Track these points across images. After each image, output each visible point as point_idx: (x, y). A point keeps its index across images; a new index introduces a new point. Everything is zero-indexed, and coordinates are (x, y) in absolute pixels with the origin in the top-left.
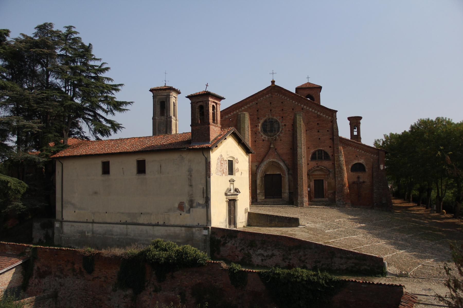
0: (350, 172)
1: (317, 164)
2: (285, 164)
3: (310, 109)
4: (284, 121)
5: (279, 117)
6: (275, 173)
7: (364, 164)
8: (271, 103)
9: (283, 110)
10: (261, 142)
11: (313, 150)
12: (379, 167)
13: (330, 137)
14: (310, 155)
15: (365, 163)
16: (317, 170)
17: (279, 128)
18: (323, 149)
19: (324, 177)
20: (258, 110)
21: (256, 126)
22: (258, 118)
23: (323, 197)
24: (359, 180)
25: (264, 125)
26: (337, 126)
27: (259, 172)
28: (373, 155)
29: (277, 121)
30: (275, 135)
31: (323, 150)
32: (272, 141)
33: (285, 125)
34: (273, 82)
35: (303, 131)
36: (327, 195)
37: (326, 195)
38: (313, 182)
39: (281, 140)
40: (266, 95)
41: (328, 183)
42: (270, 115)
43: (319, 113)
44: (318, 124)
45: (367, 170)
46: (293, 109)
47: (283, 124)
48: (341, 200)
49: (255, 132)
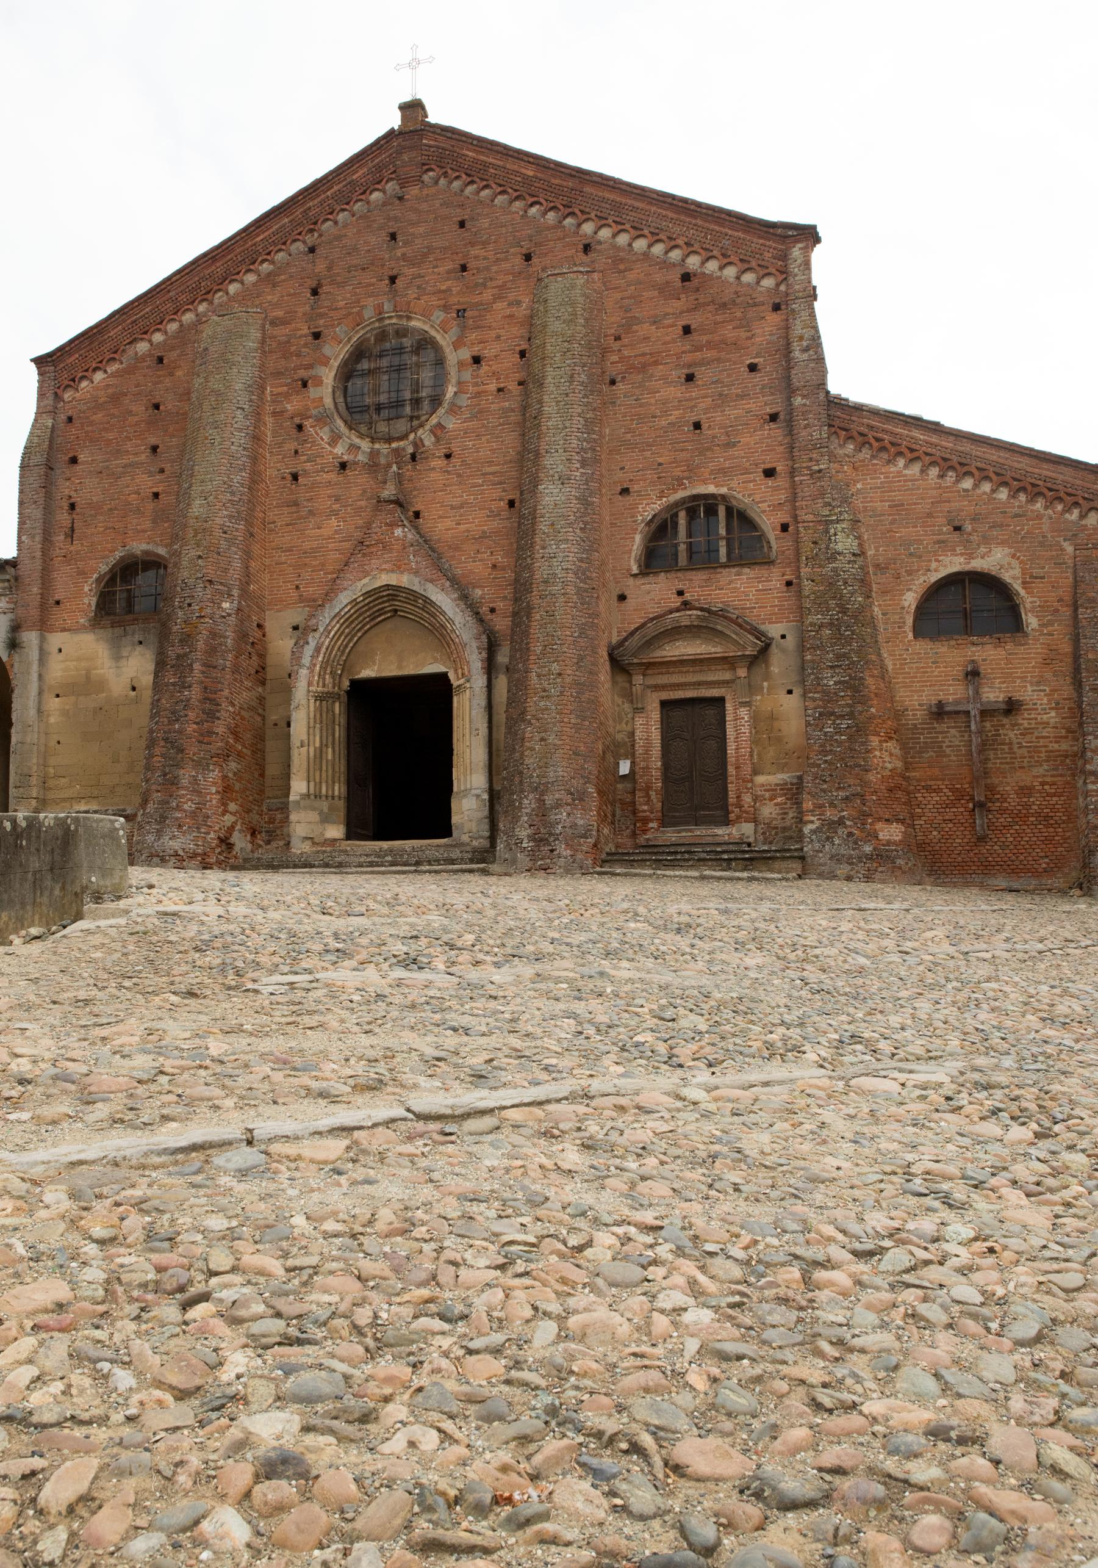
0: (911, 636)
1: (680, 593)
3: (640, 245)
4: (473, 336)
5: (439, 316)
6: (411, 669)
7: (1012, 576)
8: (393, 237)
9: (464, 268)
11: (657, 506)
14: (638, 538)
15: (1017, 572)
16: (676, 632)
17: (440, 382)
18: (724, 490)
19: (727, 676)
20: (320, 285)
21: (305, 384)
22: (317, 336)
23: (726, 822)
26: (815, 328)
27: (306, 660)
29: (425, 343)
31: (723, 497)
32: (395, 468)
33: (477, 360)
35: (583, 378)
36: (747, 799)
37: (740, 806)
38: (655, 715)
41: (755, 719)
43: (693, 262)
44: (687, 330)
45: (1031, 621)
46: (528, 258)
47: (465, 354)
49: (297, 420)
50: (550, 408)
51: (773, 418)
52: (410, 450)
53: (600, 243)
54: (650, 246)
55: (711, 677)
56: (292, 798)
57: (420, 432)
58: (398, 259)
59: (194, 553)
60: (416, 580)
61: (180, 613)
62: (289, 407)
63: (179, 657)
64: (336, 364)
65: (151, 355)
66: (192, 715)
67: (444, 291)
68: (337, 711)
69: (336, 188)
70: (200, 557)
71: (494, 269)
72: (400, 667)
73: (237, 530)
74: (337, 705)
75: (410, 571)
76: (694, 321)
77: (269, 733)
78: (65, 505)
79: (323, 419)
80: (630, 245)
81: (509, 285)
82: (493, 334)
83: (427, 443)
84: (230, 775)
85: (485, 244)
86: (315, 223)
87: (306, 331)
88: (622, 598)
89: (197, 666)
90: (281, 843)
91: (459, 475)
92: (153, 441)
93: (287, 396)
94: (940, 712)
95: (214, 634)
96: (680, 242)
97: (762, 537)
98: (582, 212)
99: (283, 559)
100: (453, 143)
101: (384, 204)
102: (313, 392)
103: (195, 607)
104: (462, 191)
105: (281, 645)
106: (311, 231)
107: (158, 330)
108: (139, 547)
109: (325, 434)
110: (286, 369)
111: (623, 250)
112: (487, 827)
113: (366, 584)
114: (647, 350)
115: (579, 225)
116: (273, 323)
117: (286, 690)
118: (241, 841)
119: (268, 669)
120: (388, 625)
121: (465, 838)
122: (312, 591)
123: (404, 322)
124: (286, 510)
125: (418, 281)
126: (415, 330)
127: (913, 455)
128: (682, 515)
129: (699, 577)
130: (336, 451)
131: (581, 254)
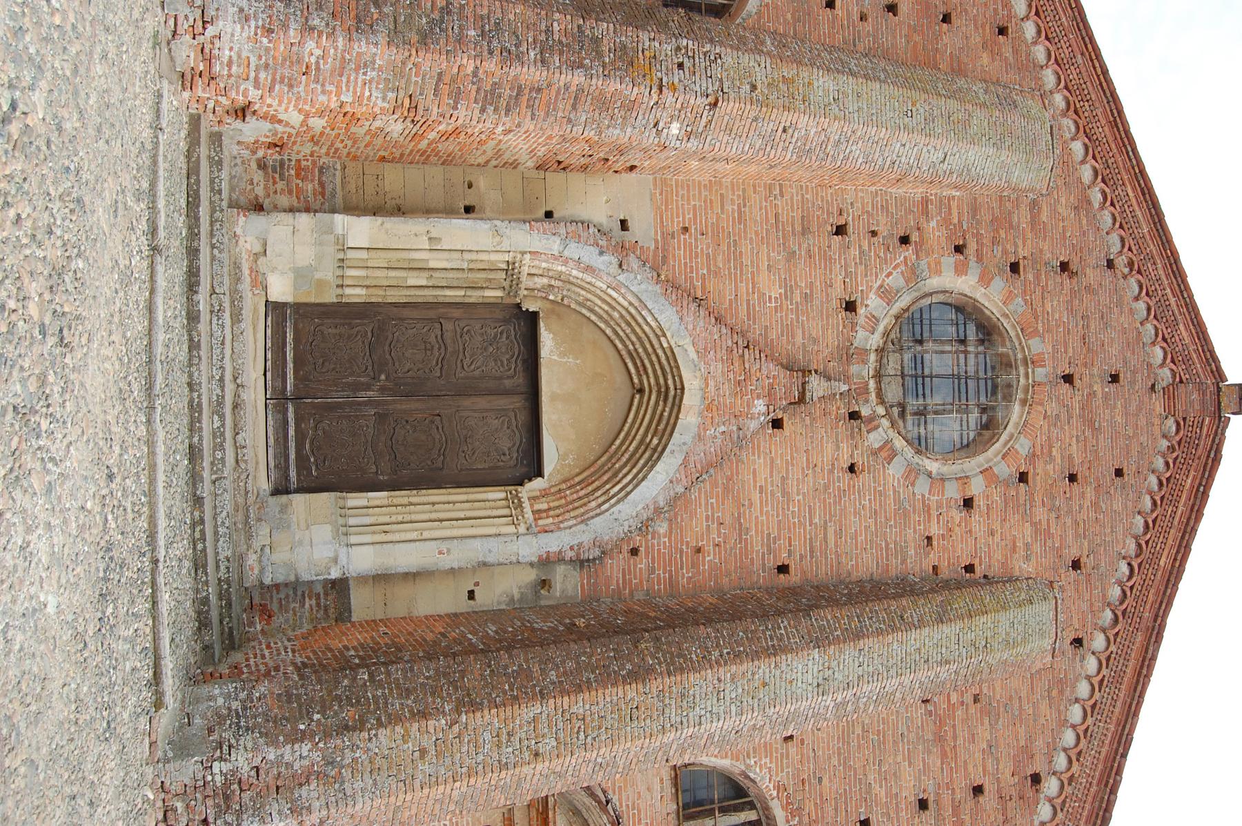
2: (645, 527)
3: (1076, 713)
5: (1023, 446)
8: (1115, 378)
10: (838, 285)
20: (1073, 274)
21: (959, 249)
27: (574, 251)
30: (888, 414)
32: (845, 388)
35: (943, 676)
42: (1039, 370)
43: (1051, 786)
44: (978, 790)
46: (1076, 565)
47: (977, 487)
49: (914, 237)
50: (915, 638)
52: (865, 412)
53: (1083, 658)
54: (1074, 727)
56: (339, 218)
57: (885, 423)
58: (1091, 386)
59: (760, 76)
60: (688, 438)
61: (668, 48)
62: (933, 224)
63: (596, 41)
64: (978, 296)
65: (1010, 17)
66: (491, 65)
67: (1050, 452)
68: (488, 293)
69: (1173, 300)
70: (754, 88)
71: (1069, 521)
72: (554, 398)
73: (786, 149)
74: (499, 293)
75: (703, 427)
76: (988, 800)
77: (457, 175)
79: (913, 275)
80: (1077, 701)
81: (1049, 543)
82: (996, 526)
83: (872, 436)
84: (378, 124)
85: (1095, 505)
86: (1139, 272)
87: (1021, 253)
90: (260, 191)
91: (826, 487)
93: (947, 221)
95: (630, 107)
96: (1076, 767)
98: (1117, 634)
99: (728, 207)
100: (1203, 459)
101: (1149, 365)
102: (950, 260)
103: (677, 76)
104: (1153, 472)
106: (1131, 264)
107: (1039, 32)
109: (896, 281)
110: (978, 222)
111: (1073, 692)
112: (280, 579)
113: (687, 357)
114: (960, 741)
115: (1104, 630)
116: (1034, 203)
119: (562, 175)
120: (620, 378)
121: (262, 534)
122: (679, 254)
123: (1020, 395)
124: (797, 215)
125: (1064, 417)
126: (1008, 409)
128: (752, 816)
130: (872, 295)
131: (1072, 636)
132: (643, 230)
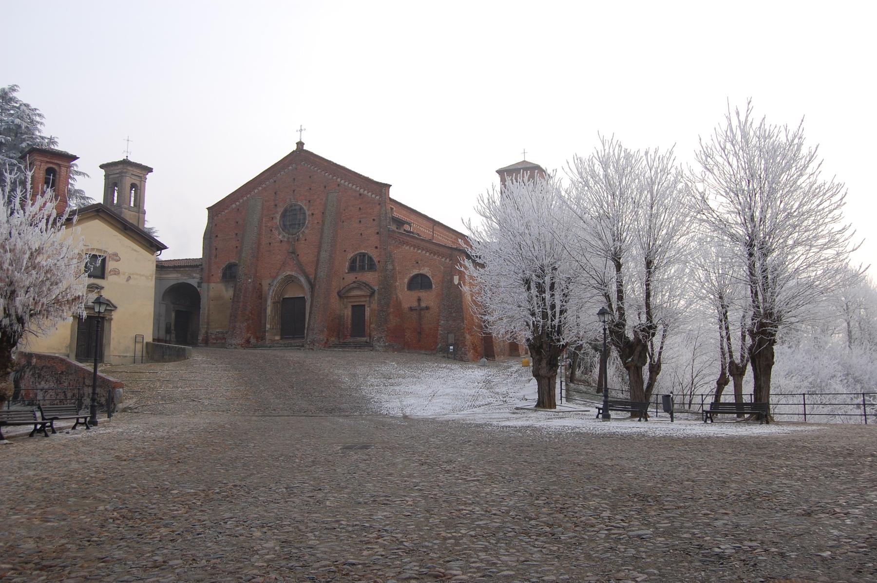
1: (356, 278)
3: (350, 185)
5: (304, 202)
8: (294, 179)
12: (452, 280)
13: (376, 231)
16: (353, 289)
17: (305, 219)
19: (365, 300)
23: (364, 336)
24: (419, 304)
25: (283, 215)
27: (271, 294)
28: (443, 260)
29: (301, 208)
33: (313, 214)
34: (300, 144)
38: (350, 309)
39: (306, 240)
40: (288, 166)
44: (360, 208)
45: (434, 286)
46: (325, 187)
47: (310, 213)
48: (382, 340)
51: (378, 233)
55: (362, 300)
56: (267, 329)
78: (214, 248)
79: (277, 228)
88: (344, 279)
89: (242, 297)
92: (236, 232)
94: (411, 309)
97: (374, 264)
102: (274, 221)
105: (265, 287)
108: (232, 261)
115: (337, 179)
117: (266, 300)
118: (253, 341)
127: (407, 244)
129: (360, 274)
132: (269, 281)
